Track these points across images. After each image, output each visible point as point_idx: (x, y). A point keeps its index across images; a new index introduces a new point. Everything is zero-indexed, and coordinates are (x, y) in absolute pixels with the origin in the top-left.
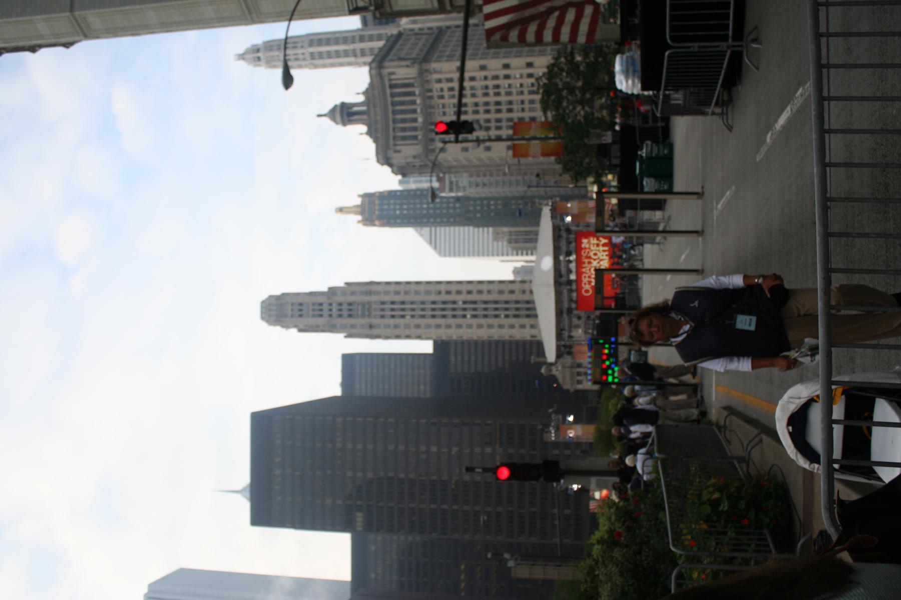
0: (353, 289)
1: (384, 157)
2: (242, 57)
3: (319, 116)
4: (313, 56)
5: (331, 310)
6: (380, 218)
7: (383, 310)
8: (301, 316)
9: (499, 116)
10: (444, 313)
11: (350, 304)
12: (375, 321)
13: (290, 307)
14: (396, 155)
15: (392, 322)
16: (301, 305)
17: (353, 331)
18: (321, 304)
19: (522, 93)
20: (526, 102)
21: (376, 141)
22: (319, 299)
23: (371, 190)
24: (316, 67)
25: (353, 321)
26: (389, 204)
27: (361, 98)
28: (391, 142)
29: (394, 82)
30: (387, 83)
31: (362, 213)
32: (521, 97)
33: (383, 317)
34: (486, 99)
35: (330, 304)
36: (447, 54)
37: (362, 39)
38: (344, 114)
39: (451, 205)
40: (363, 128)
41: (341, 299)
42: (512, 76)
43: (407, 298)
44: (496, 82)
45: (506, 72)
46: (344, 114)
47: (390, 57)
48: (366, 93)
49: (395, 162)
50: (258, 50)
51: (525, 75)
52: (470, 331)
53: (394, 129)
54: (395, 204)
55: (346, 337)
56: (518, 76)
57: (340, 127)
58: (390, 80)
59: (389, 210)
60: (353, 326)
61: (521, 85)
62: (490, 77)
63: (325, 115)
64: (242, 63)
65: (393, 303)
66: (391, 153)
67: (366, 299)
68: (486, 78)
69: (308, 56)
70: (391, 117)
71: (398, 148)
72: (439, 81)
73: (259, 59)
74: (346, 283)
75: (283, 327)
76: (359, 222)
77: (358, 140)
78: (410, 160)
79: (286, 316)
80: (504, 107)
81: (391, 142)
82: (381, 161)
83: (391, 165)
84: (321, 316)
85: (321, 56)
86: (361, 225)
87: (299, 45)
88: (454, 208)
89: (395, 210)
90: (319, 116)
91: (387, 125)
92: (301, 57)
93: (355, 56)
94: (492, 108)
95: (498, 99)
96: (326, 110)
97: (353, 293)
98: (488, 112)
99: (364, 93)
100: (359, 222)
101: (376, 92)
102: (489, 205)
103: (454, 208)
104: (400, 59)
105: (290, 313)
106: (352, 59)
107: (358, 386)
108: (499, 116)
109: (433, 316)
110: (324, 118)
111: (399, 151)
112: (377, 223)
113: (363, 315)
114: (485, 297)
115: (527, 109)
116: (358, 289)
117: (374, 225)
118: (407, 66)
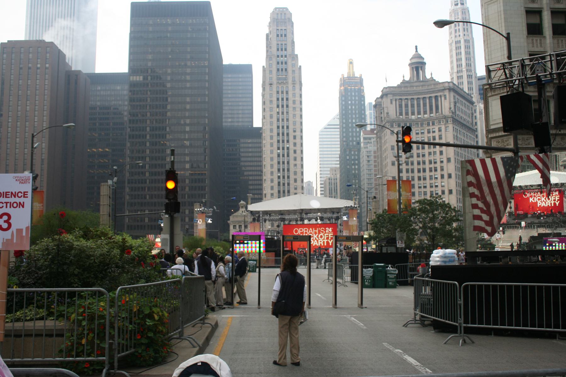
0: (297, 72)
1: (387, 93)
3: (416, 47)
4: (458, 42)
5: (282, 56)
6: (346, 90)
7: (282, 92)
8: (278, 36)
9: (416, 171)
10: (281, 135)
11: (286, 70)
12: (274, 86)
13: (284, 28)
14: (389, 101)
15: (275, 99)
16: (285, 35)
17: (267, 72)
18: (286, 50)
19: (431, 187)
20: (425, 190)
21: (399, 86)
22: (289, 49)
23: (365, 84)
24: (450, 45)
25: (275, 71)
26: (355, 96)
27: (428, 76)
28: (398, 97)
29: (439, 99)
30: (438, 94)
31: (349, 78)
32: (428, 186)
33: (278, 92)
34: (427, 162)
35: (286, 56)
36: (459, 135)
37: (469, 76)
38: (418, 65)
39: (355, 139)
40: (407, 78)
41: (289, 63)
42: (443, 180)
43: (291, 109)
44: (439, 169)
45: (446, 176)
46: (418, 65)
47: (457, 96)
48: (432, 79)
49: (384, 99)
50: (462, 4)
51: (443, 189)
52: (269, 152)
53: (407, 99)
54: (355, 100)
55: (263, 67)
56: (443, 184)
57: (409, 62)
58: (441, 96)
59: (351, 96)
60: (271, 72)
61: (437, 186)
62: (442, 165)
63: (417, 51)
65: (287, 99)
66: (390, 97)
67: (290, 81)
68: (442, 162)
69: (458, 39)
70: (416, 97)
71: (394, 102)
72: (440, 130)
73: (457, 5)
74: (300, 66)
75: (270, 23)
76: (343, 75)
77: (399, 74)
78: (386, 111)
79: (277, 26)
80: (421, 174)
81: (398, 97)
82: (384, 91)
83: (382, 97)
84: (278, 50)
85: (458, 48)
86: (341, 77)
87: (466, 33)
88: (353, 141)
89: (351, 100)
90: (416, 47)
91: (410, 94)
92: (457, 34)
93: (458, 72)
94: (421, 167)
95: (427, 170)
96: (420, 52)
97: (293, 71)
98: (419, 163)
99: (432, 78)
100: (343, 75)
102: (354, 164)
103: (353, 141)
104: (455, 103)
105: (280, 28)
106: (455, 70)
107: (230, 76)
108: (416, 171)
109: (278, 127)
110: (415, 50)
111: (391, 103)
112: (342, 88)
113: (278, 79)
114: (292, 162)
115: (420, 190)
116: (297, 75)
117: (341, 87)
118: (450, 108)
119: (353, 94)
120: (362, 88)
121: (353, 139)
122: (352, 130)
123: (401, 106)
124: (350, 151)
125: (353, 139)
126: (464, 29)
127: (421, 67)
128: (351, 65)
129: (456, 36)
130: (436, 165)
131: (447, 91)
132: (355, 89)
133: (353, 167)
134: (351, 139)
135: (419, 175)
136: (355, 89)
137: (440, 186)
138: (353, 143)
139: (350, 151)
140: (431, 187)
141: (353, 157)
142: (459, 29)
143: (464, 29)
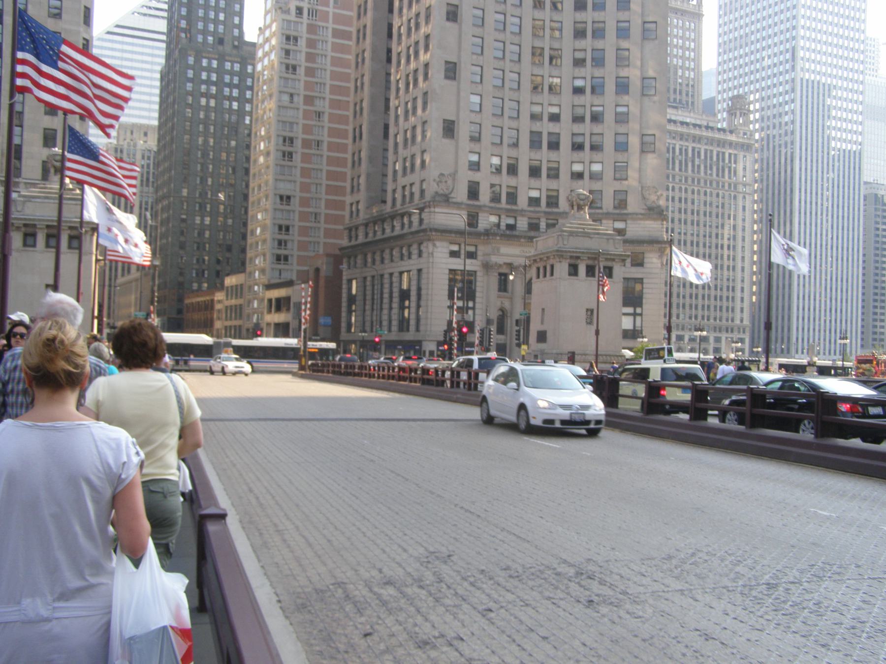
20: (553, 127)
32: (566, 117)
39: (211, 27)
61: (596, 118)
88: (205, 32)
103: (205, 32)
121: (206, 26)
125: (206, 26)
130: (599, 44)
133: (203, 101)
134: (200, 25)
138: (205, 39)
140: (578, 119)
141: (204, 76)
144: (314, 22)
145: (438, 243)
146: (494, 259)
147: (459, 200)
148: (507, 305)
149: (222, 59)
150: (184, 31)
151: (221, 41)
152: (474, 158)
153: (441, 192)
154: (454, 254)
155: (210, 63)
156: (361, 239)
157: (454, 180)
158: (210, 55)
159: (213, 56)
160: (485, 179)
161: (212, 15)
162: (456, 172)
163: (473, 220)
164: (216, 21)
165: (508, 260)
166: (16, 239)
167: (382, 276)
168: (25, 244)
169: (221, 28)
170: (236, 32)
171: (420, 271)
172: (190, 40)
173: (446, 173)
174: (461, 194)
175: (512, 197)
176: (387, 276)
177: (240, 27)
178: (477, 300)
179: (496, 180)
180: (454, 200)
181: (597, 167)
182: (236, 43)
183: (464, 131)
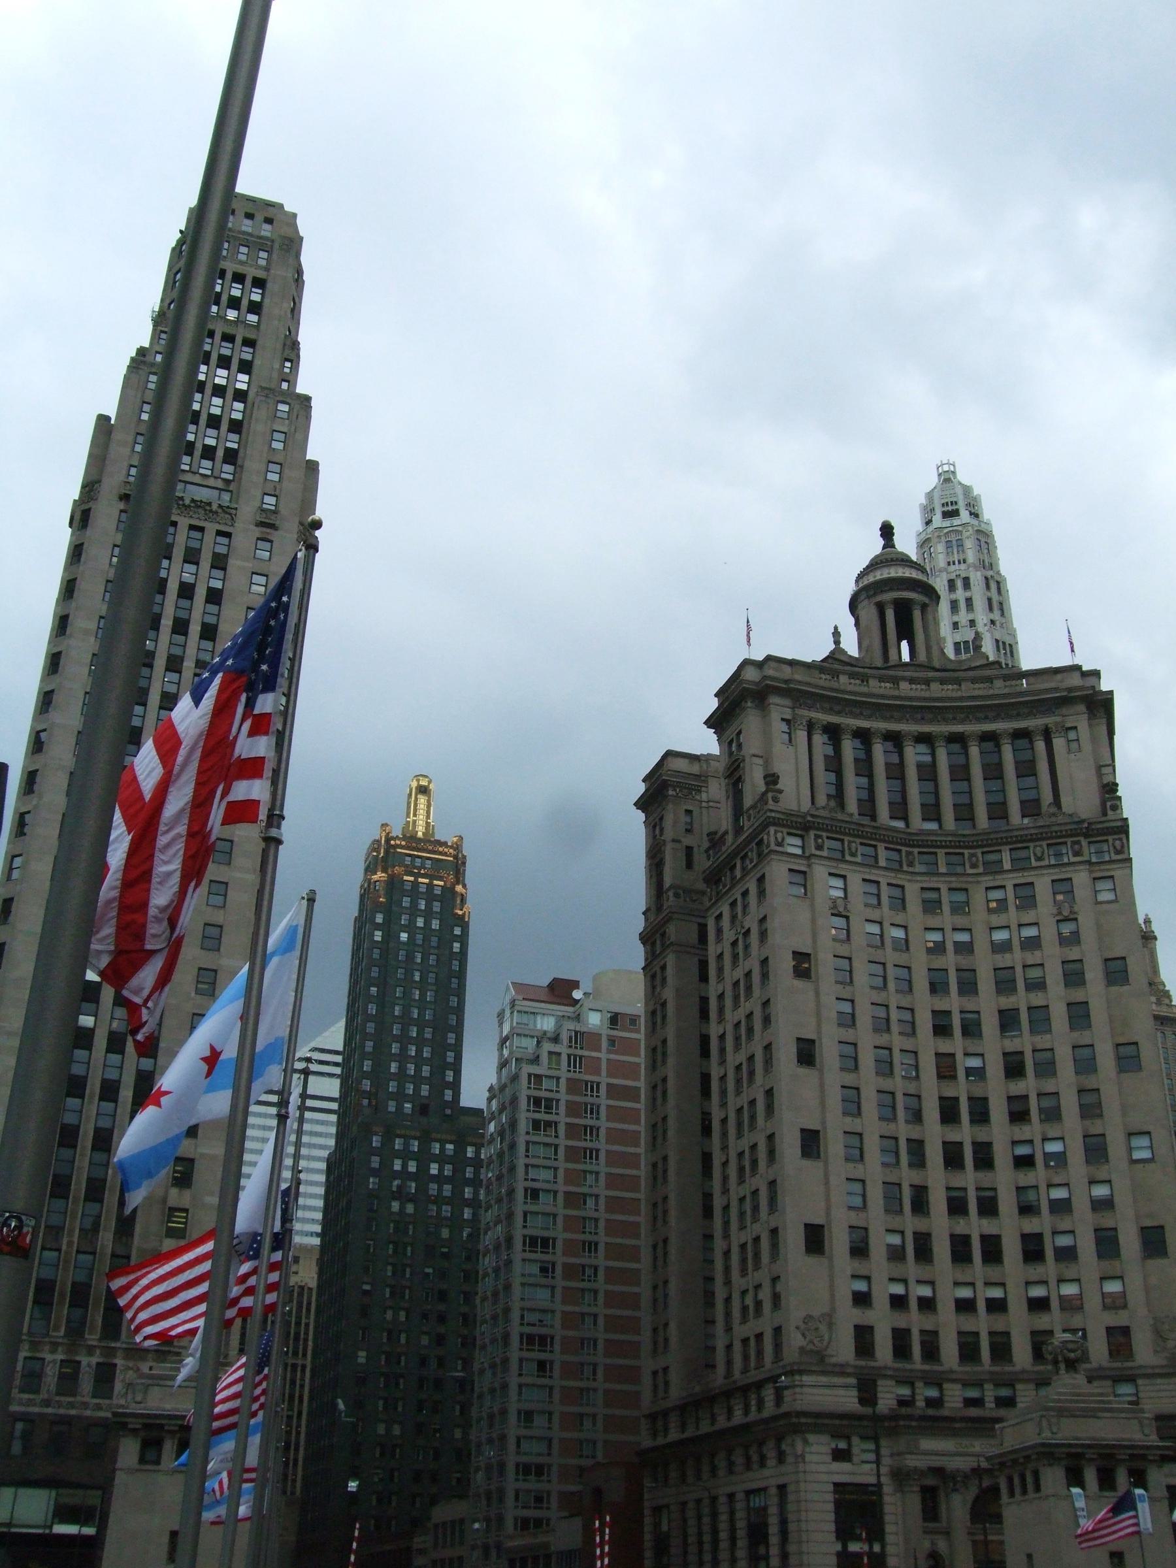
2: (947, 478)
6: (393, 884)
19: (1026, 1209)
39: (410, 1089)
44: (1070, 1104)
58: (1047, 735)
64: (932, 481)
66: (779, 708)
86: (377, 833)
88: (400, 1096)
89: (410, 928)
101: (999, 687)
103: (400, 1096)
110: (881, 542)
117: (370, 869)
119: (422, 905)
120: (459, 888)
121: (401, 1087)
122: (403, 1049)
123: (835, 764)
124: (388, 1137)
125: (401, 1087)
126: (990, 600)
127: (924, 607)
128: (422, 800)
129: (955, 625)
131: (1082, 708)
132: (430, 886)
134: (392, 1086)
135: (954, 1136)
136: (430, 886)
137: (1081, 1205)
138: (400, 1108)
139: (388, 1137)
142: (969, 601)
143: (990, 600)
144: (577, 1076)
145: (811, 1438)
146: (912, 1462)
147: (841, 1359)
148: (942, 1546)
149: (426, 1139)
150: (369, 1095)
151: (423, 1109)
152: (861, 1286)
153: (811, 1347)
154: (840, 1455)
155: (406, 1145)
156: (674, 1435)
157: (830, 1325)
158: (408, 1133)
159: (413, 1133)
160: (882, 1320)
161: (411, 1069)
162: (833, 1309)
163: (867, 1393)
164: (417, 1080)
165: (937, 1462)
166: (128, 1451)
167: (714, 1499)
168: (142, 1460)
169: (425, 1090)
170: (448, 1095)
171: (782, 1488)
172: (377, 1108)
173: (816, 1313)
174: (844, 1349)
175: (931, 1351)
176: (723, 1500)
177: (456, 1086)
178: (890, 1539)
179: (901, 1321)
180: (833, 1360)
181: (1069, 1290)
182: (448, 1112)
183: (839, 1241)
